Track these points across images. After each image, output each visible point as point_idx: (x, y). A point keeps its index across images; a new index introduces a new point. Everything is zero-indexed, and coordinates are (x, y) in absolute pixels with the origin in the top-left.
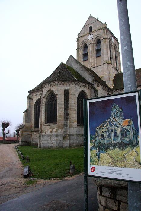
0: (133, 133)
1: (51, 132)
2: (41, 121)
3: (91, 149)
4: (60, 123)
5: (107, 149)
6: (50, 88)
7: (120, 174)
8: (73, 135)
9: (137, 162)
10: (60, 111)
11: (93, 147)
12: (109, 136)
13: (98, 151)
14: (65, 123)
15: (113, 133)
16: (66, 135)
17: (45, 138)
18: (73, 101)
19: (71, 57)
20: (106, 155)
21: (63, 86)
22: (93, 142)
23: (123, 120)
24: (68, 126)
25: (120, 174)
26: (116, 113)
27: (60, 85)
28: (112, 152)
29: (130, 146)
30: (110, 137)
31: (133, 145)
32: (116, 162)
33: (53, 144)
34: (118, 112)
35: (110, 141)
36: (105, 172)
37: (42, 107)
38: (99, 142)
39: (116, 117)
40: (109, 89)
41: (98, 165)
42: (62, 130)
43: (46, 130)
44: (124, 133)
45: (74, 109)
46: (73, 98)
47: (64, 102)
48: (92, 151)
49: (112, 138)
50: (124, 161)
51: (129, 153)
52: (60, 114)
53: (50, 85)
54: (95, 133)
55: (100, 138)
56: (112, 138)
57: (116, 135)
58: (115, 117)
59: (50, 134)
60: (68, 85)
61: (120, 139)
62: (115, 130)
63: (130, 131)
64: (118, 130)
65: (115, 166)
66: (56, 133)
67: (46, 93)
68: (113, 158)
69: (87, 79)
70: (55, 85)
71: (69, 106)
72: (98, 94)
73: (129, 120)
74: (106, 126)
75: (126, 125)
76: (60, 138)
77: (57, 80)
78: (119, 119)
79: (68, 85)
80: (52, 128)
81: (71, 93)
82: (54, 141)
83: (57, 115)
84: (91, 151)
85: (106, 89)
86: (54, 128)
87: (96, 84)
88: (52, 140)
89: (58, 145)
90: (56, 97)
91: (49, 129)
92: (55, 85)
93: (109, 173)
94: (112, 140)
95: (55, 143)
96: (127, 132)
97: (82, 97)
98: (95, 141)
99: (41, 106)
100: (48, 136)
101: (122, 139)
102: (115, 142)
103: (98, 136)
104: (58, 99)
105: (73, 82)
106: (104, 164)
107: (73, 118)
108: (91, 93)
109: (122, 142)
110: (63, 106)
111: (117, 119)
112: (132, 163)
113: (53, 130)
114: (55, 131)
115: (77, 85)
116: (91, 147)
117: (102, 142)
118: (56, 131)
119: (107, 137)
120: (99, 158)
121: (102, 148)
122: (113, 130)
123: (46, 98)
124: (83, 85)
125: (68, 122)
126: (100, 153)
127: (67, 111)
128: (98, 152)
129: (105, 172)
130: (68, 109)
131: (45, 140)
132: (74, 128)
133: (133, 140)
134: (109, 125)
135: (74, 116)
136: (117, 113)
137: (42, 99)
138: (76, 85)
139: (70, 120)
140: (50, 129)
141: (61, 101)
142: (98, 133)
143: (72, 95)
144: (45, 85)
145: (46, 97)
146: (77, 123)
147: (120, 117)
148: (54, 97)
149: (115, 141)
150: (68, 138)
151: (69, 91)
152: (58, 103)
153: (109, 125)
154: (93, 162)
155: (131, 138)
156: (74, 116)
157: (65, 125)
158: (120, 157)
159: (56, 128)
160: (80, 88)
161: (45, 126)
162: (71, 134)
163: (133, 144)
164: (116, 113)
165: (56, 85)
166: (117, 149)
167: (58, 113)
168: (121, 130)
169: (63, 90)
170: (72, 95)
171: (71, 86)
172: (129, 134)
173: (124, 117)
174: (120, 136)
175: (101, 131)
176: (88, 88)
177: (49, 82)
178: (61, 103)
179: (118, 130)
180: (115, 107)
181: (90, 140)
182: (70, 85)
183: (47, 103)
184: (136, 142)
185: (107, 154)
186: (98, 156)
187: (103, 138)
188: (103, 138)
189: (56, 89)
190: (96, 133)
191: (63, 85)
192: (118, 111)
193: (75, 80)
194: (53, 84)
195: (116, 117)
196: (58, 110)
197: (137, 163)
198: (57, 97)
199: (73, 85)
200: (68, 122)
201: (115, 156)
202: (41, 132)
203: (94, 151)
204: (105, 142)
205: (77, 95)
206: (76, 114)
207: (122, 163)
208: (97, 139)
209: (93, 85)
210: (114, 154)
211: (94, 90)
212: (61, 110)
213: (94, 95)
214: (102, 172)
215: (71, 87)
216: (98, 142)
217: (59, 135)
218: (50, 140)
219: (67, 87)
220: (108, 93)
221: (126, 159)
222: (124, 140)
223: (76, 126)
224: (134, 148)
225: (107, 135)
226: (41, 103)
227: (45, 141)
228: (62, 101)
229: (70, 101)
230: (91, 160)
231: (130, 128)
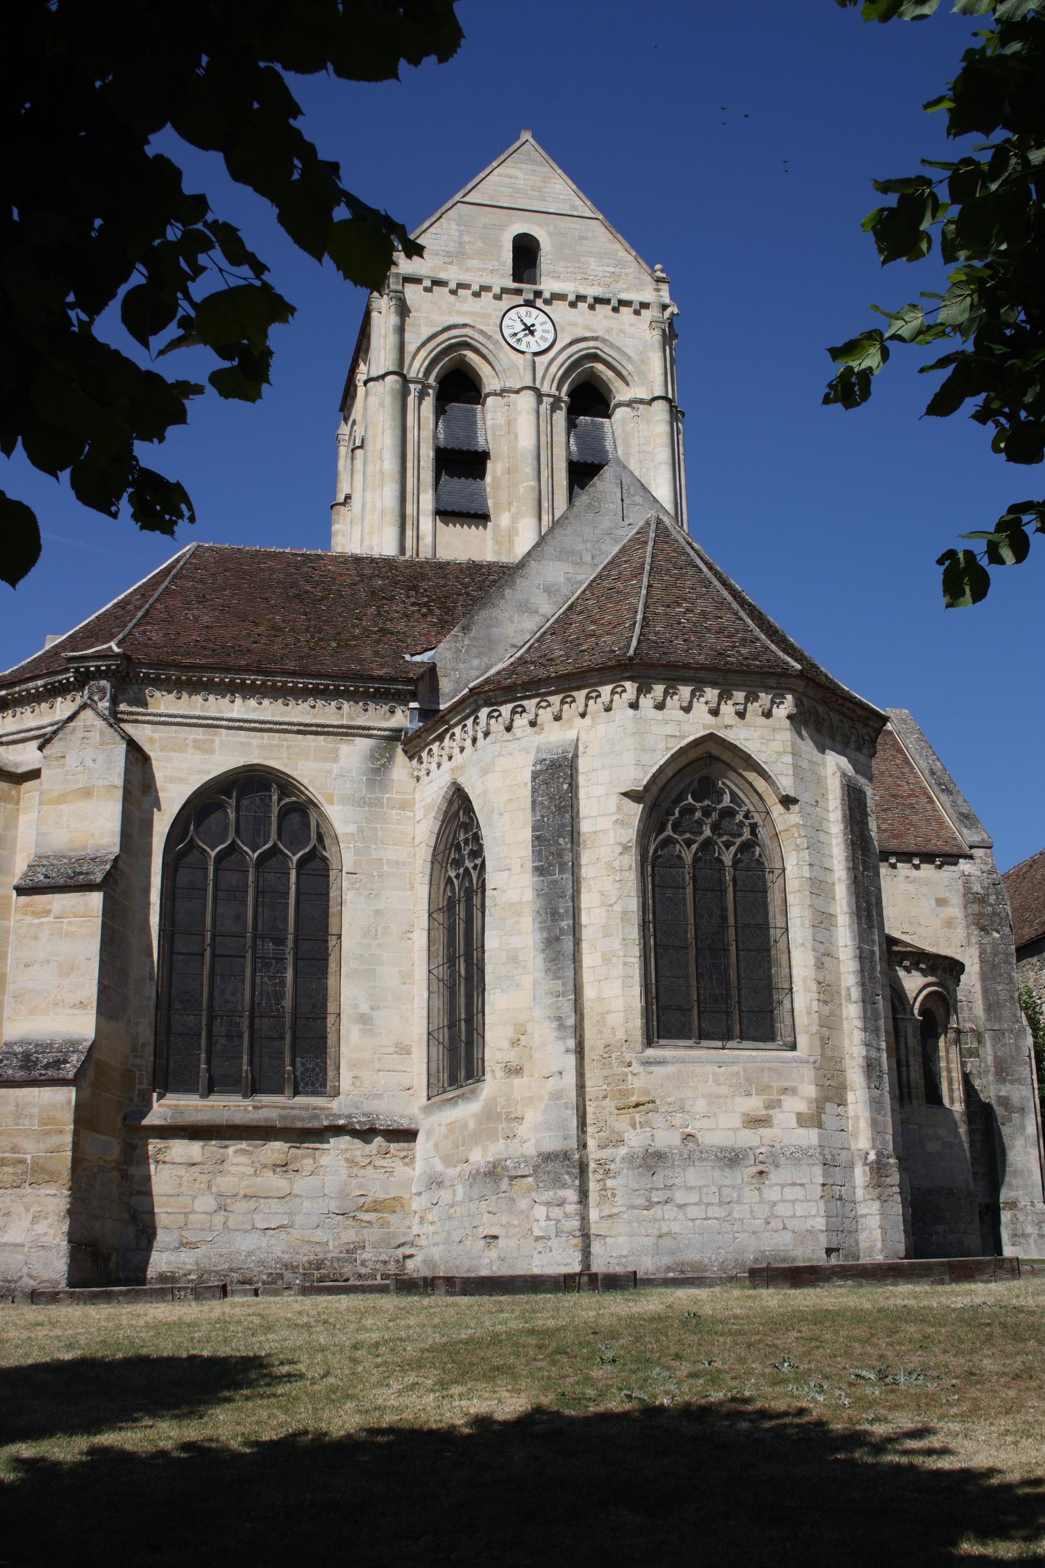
1: (755, 1122)
6: (710, 719)
17: (692, 1176)
43: (701, 1106)
59: (748, 1138)
80: (763, 1090)
82: (800, 1209)
88: (772, 1194)
95: (820, 1223)
100: (732, 1158)
113: (774, 1104)
114: (799, 1115)
118: (802, 1120)
123: (650, 798)
131: (694, 1197)
140: (749, 1095)
148: (728, 813)
218: (750, 1195)
227: (693, 1212)
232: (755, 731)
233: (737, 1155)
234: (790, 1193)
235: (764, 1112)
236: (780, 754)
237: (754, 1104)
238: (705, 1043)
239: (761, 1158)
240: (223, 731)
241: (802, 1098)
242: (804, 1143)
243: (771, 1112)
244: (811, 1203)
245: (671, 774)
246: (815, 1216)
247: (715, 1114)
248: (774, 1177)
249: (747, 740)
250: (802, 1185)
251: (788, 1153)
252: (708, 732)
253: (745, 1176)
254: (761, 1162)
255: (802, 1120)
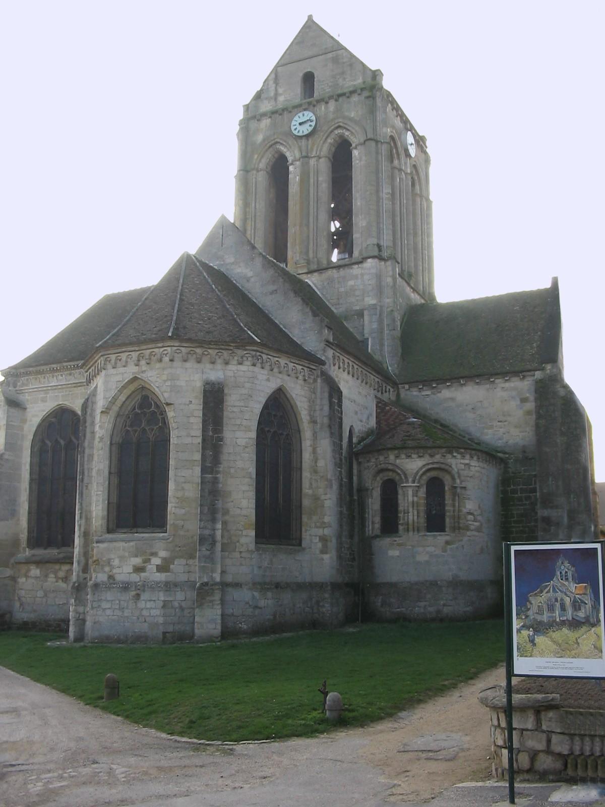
0: (592, 605)
1: (139, 569)
2: (88, 520)
3: (519, 631)
4: (182, 533)
5: (547, 630)
6: (135, 369)
7: (571, 668)
8: (237, 585)
9: (597, 649)
10: (182, 480)
11: (523, 626)
12: (551, 608)
13: (531, 633)
14: (207, 532)
15: (558, 605)
16: (206, 584)
18: (239, 434)
19: (223, 220)
20: (546, 639)
21: (197, 366)
22: (522, 619)
23: (576, 585)
24: (219, 546)
25: (571, 668)
26: (563, 573)
27: (185, 361)
28: (557, 635)
29: (587, 625)
30: (553, 610)
31: (592, 624)
32: (563, 650)
33: (146, 625)
34: (567, 570)
35: (552, 617)
36: (545, 668)
37: (91, 456)
38: (534, 618)
39: (564, 579)
40: (386, 377)
41: (531, 656)
42: (191, 562)
43: (116, 562)
44: (577, 605)
45: (243, 469)
46: (238, 422)
47: (204, 440)
48: (520, 632)
49: (557, 612)
50: (577, 648)
51: (585, 636)
52: (183, 489)
53: (135, 355)
54: (526, 604)
55: (536, 612)
56: (557, 612)
57: (563, 608)
58: (562, 579)
59: (135, 578)
60: (219, 361)
61: (570, 613)
62: (562, 600)
63: (587, 602)
64: (567, 601)
65: (562, 657)
66: (161, 577)
67: (113, 393)
68: (559, 645)
69: (296, 335)
70: (161, 361)
71: (224, 457)
72: (340, 406)
73: (586, 586)
74: (547, 593)
75: (581, 592)
76: (180, 596)
77: (171, 338)
78: (569, 583)
79: (219, 361)
81: (233, 400)
83: (170, 494)
84: (519, 634)
85: (373, 378)
86: (155, 554)
87: (334, 357)
89: (170, 629)
90: (163, 413)
91: (127, 554)
92: (161, 361)
93: (552, 668)
94: (557, 616)
96: (582, 604)
97: (275, 416)
98: (527, 617)
99: (87, 451)
100: (126, 587)
101: (574, 614)
102: (561, 619)
103: (531, 609)
104: (172, 425)
105: (240, 352)
106: (542, 654)
107: (238, 511)
108: (312, 402)
109: (573, 618)
110: (198, 456)
111: (566, 583)
112: (589, 650)
113: (147, 561)
115: (259, 365)
116: (518, 627)
117: (539, 618)
118: (160, 569)
119: (548, 610)
120: (534, 645)
121: (539, 628)
122: (559, 599)
124: (282, 364)
125: (219, 526)
126: (536, 636)
127: (215, 481)
128: (531, 635)
129: (545, 668)
130: (218, 472)
132: (243, 555)
133: (591, 616)
134: (551, 591)
135: (244, 503)
136: (566, 572)
137: (93, 417)
138: (254, 365)
139: (227, 518)
140: (136, 556)
141: (188, 435)
142: (531, 604)
143: (235, 409)
144: (113, 357)
145: (115, 408)
146: (253, 533)
147: (570, 579)
148: (154, 412)
149: (562, 616)
150: (217, 596)
151: (226, 391)
152: (174, 441)
153: (551, 591)
154: (523, 651)
155: (588, 614)
156: (244, 503)
157: (206, 540)
158: (570, 642)
159: (163, 554)
160: (268, 380)
161: (111, 541)
162: (229, 579)
163: (590, 622)
164: (563, 573)
165: (166, 359)
166: (565, 630)
167: (172, 486)
168: (572, 600)
169: (199, 384)
170: (235, 409)
171: (233, 367)
172: (585, 607)
173: (579, 579)
174: (570, 611)
175: (537, 601)
176: (301, 377)
177: (131, 344)
178: (188, 440)
179: (567, 601)
180: (562, 563)
181: (517, 614)
182: (227, 363)
183: (118, 439)
184: (595, 620)
185: (547, 637)
186: (532, 641)
187: (540, 611)
188: (540, 611)
189: (164, 377)
190: (528, 603)
191: (199, 361)
192: (568, 569)
193: (253, 343)
194: (151, 354)
195: (564, 579)
196: (171, 473)
197: (596, 651)
198: (170, 414)
199: (240, 364)
200: (219, 526)
201: (562, 640)
202: (85, 569)
203: (525, 633)
204: (545, 618)
205: (258, 408)
206: (252, 495)
207: (573, 652)
208: (530, 613)
209: (323, 363)
210: (559, 638)
211: (326, 389)
212: (186, 473)
213: (326, 408)
214: (540, 667)
215: (230, 374)
216: (532, 618)
217: (176, 585)
219: (215, 374)
220: (379, 395)
221: (581, 645)
222: (577, 616)
223: (252, 546)
224: (593, 629)
225: (548, 608)
226: (88, 435)
228: (193, 433)
229: (228, 434)
230: (518, 649)
231: (586, 597)
232: (155, 371)
233: (128, 586)
234: (149, 605)
235: (143, 565)
236: (165, 381)
237: (137, 561)
238: (135, 530)
239: (139, 587)
240: (50, 392)
241: (160, 558)
242: (158, 579)
243: (145, 565)
244: (157, 610)
245: (124, 399)
246: (159, 616)
247: (122, 567)
248: (142, 597)
249: (150, 377)
250: (154, 601)
251: (149, 585)
252: (134, 376)
253: (131, 597)
254: (139, 589)
255: (160, 569)
